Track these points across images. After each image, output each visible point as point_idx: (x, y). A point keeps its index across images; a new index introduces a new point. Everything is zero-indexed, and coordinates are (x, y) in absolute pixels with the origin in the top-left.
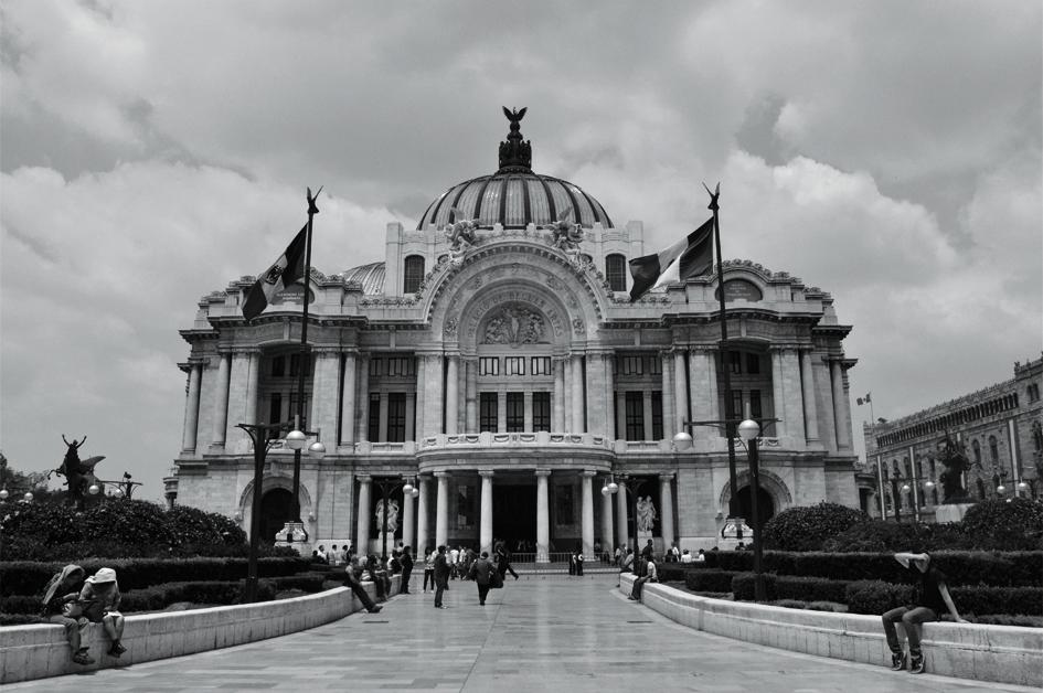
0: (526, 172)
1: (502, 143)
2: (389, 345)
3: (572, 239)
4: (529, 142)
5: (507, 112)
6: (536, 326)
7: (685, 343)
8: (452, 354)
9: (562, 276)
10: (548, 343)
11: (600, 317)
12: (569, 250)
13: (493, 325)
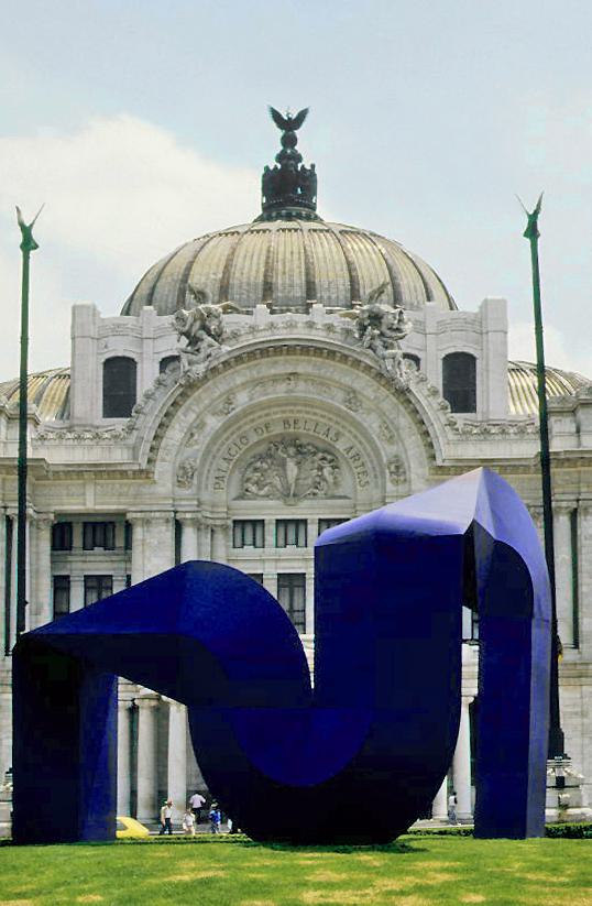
0: (308, 218)
1: (267, 168)
2: (84, 504)
3: (388, 333)
4: (313, 166)
5: (276, 116)
6: (327, 471)
7: (573, 497)
8: (188, 516)
9: (369, 393)
10: (345, 497)
11: (434, 457)
12: (381, 351)
13: (256, 470)
